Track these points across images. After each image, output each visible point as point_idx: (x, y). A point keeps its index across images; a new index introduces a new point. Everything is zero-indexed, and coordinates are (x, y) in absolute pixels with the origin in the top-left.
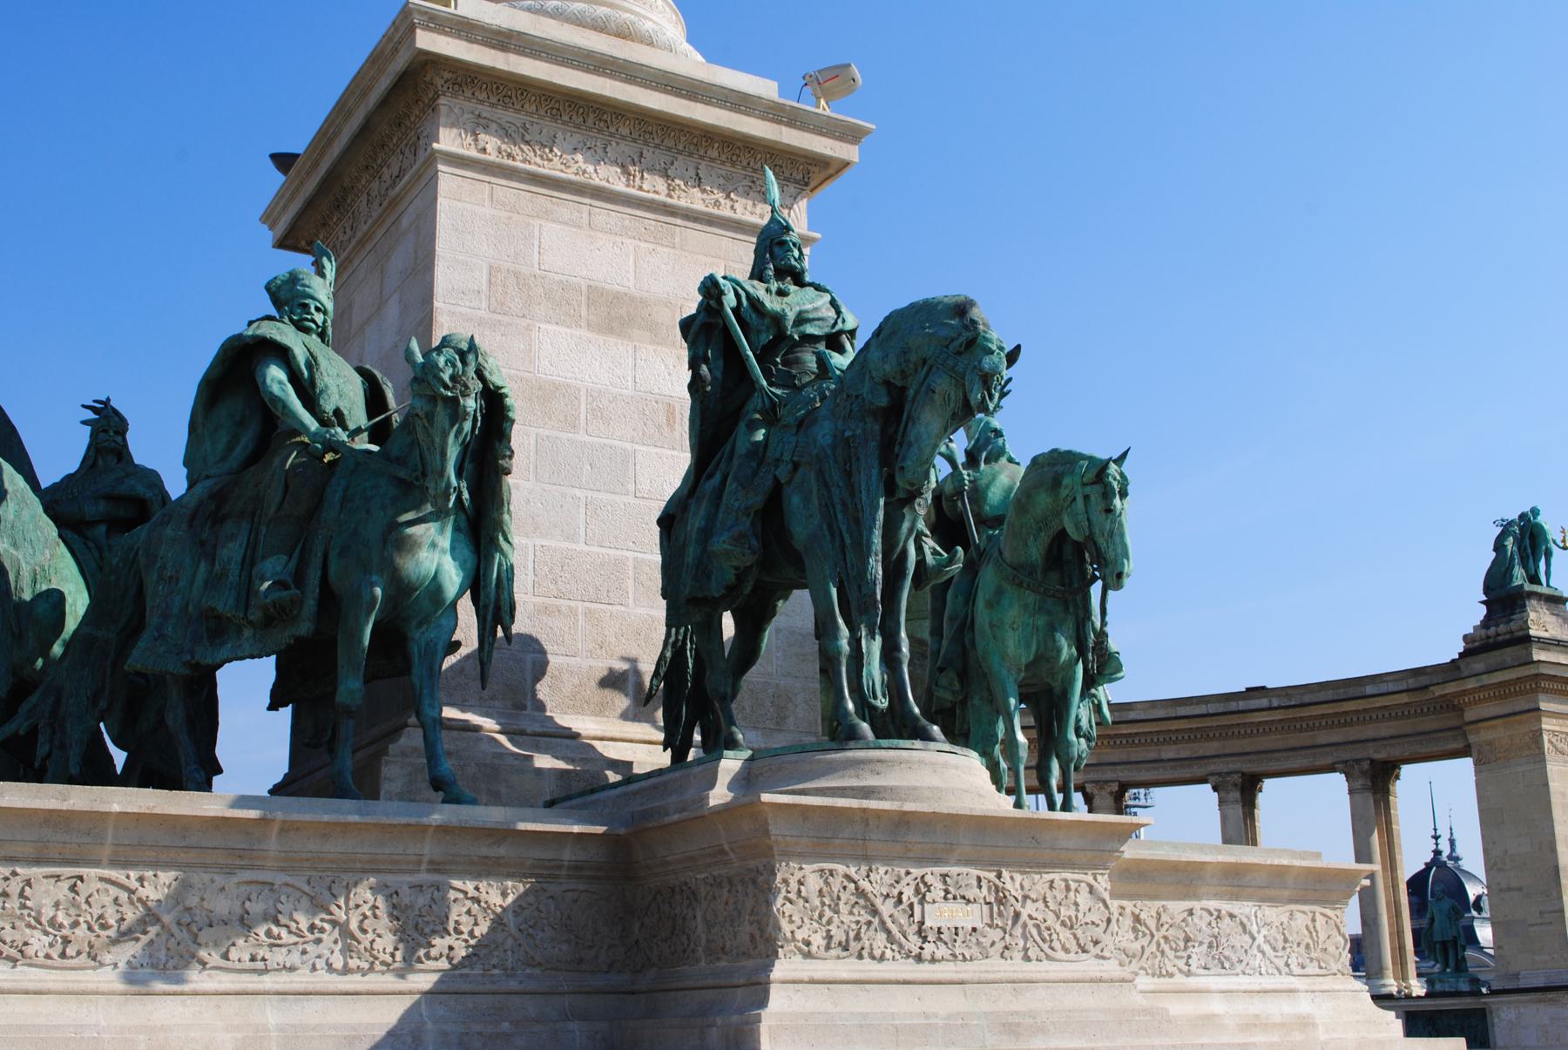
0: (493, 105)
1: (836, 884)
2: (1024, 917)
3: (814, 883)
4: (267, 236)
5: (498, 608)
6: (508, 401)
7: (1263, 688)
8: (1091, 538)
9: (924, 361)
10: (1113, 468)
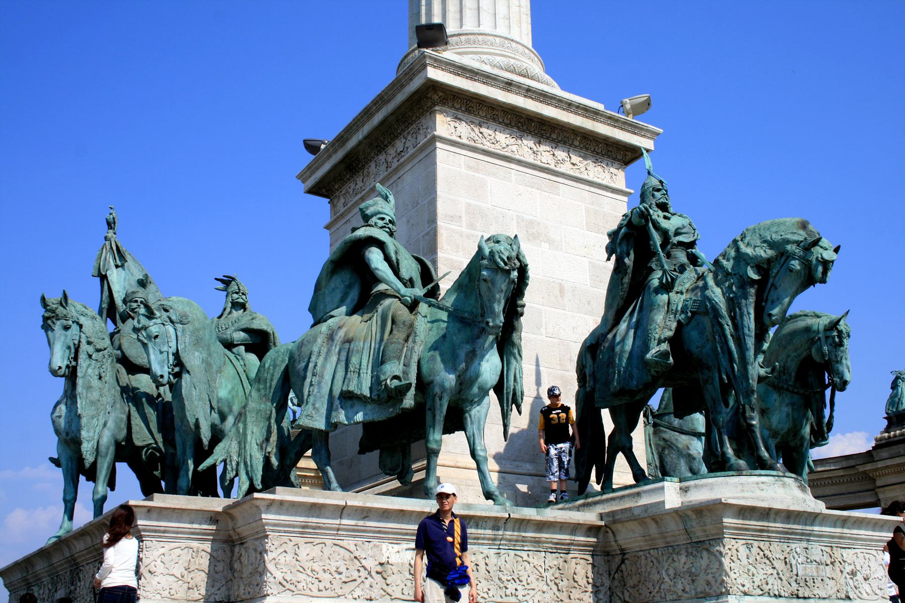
0: (462, 111)
3: (743, 551)
4: (302, 187)
5: (514, 394)
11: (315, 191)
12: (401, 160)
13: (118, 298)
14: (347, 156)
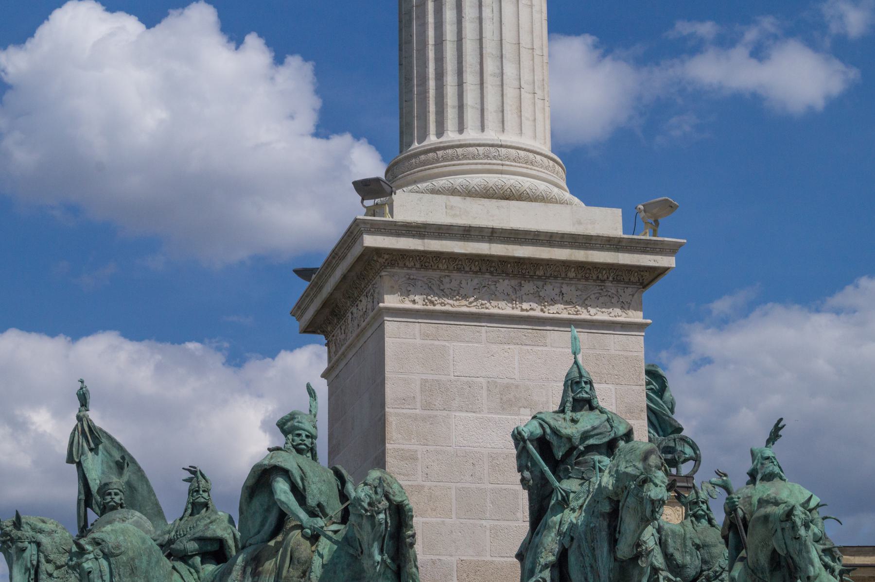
13: (94, 487)
14: (325, 304)
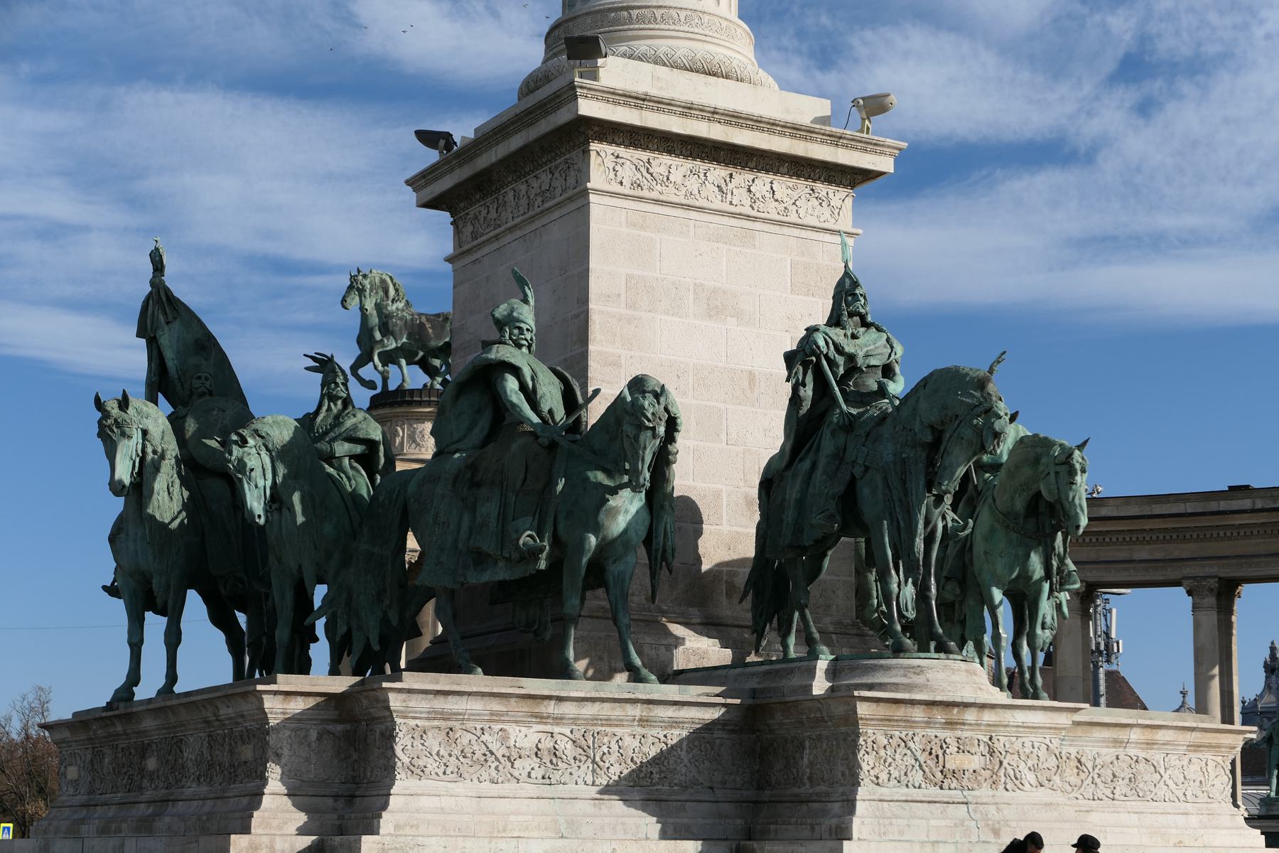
1: (894, 742)
2: (1005, 764)
5: (664, 551)
6: (678, 421)
7: (1247, 487)
8: (1059, 501)
9: (957, 416)
10: (1077, 453)
11: (432, 204)
12: (547, 205)
